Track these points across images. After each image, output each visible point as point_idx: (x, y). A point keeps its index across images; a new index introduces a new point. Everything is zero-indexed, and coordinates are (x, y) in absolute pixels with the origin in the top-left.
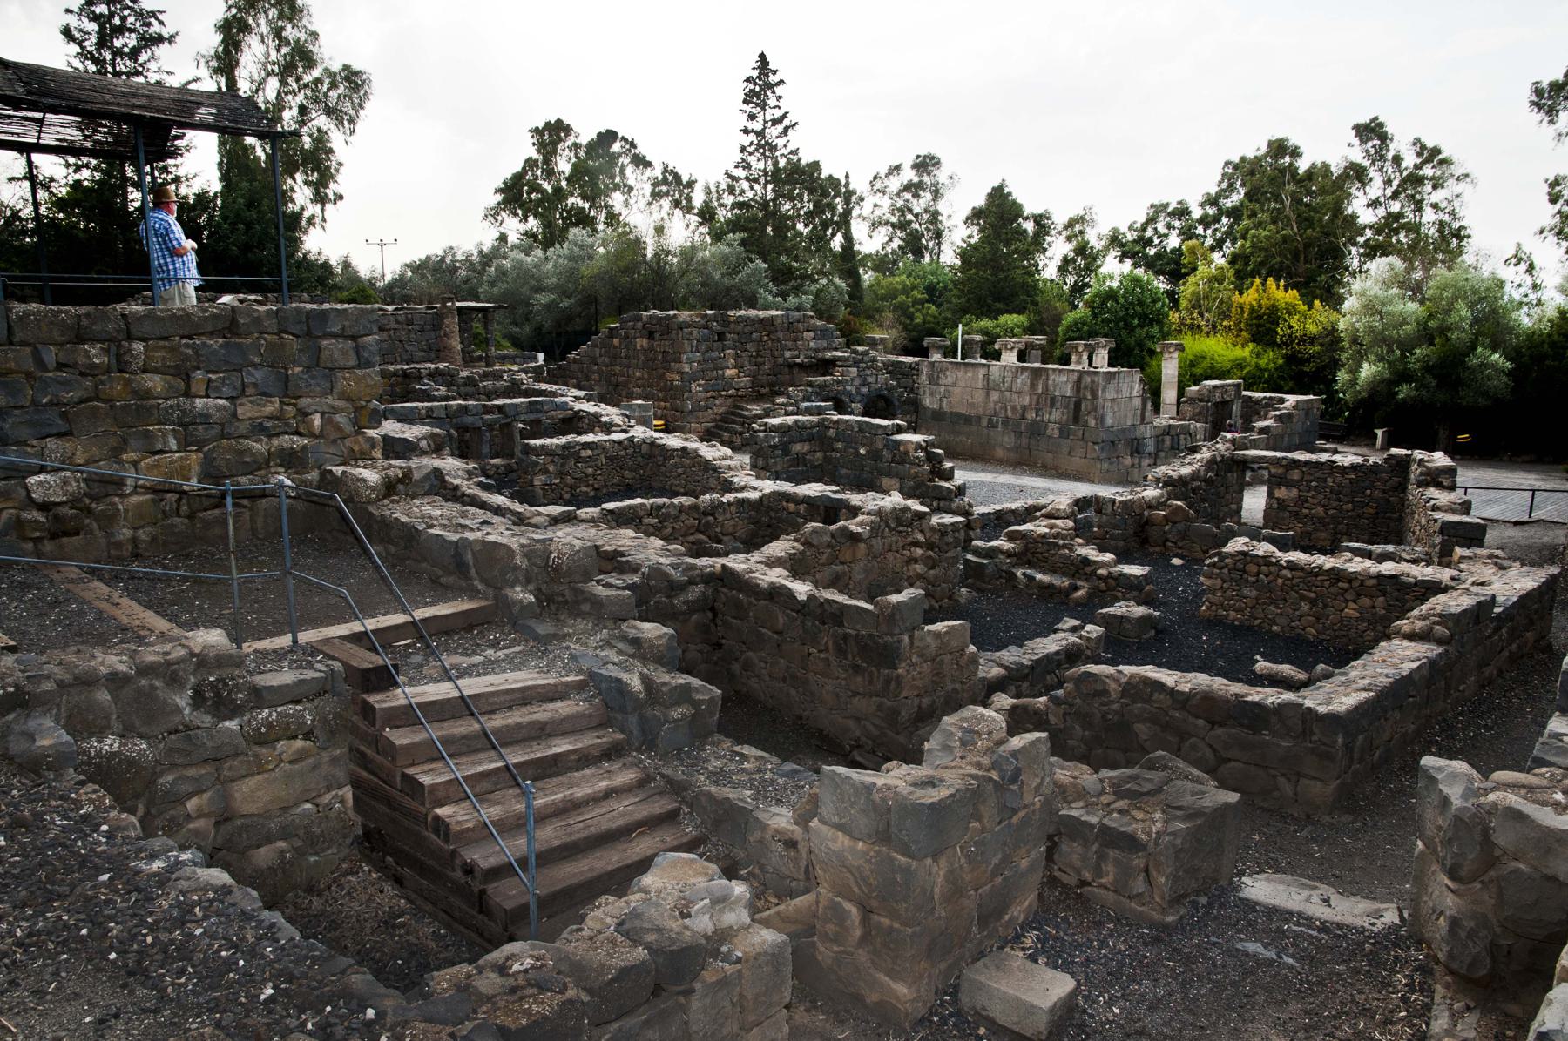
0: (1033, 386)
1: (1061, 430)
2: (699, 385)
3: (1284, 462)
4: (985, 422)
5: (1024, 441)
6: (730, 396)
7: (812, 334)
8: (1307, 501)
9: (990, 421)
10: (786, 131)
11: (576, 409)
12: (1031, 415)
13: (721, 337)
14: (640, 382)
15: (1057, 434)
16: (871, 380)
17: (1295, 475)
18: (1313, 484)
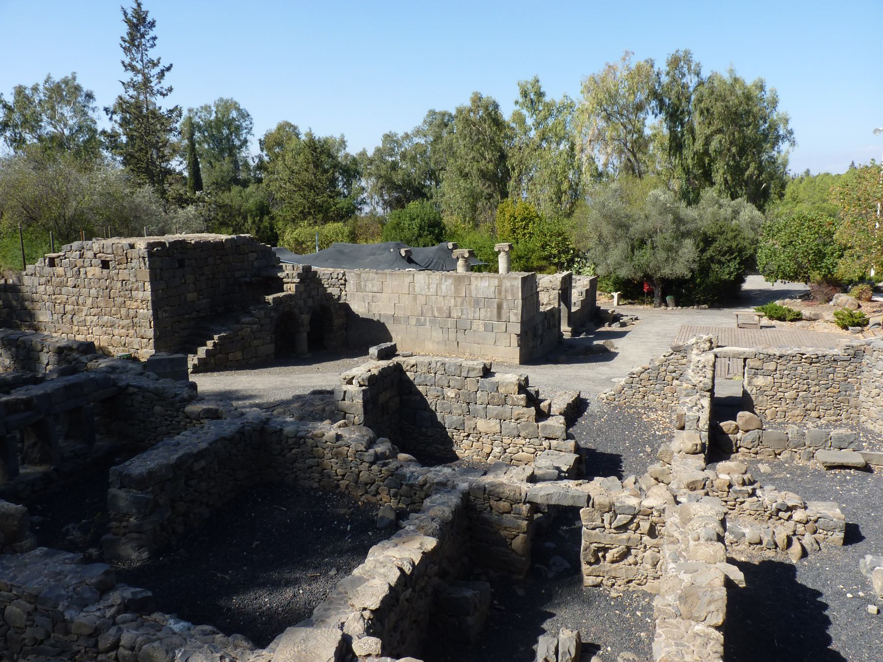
0: (457, 290)
1: (485, 325)
2: (165, 311)
3: (762, 356)
4: (413, 321)
5: (452, 336)
6: (193, 319)
7: (255, 255)
8: (781, 387)
9: (418, 320)
10: (161, 75)
11: (122, 384)
12: (455, 314)
13: (181, 264)
14: (94, 311)
15: (482, 328)
16: (314, 293)
17: (771, 366)
18: (786, 372)
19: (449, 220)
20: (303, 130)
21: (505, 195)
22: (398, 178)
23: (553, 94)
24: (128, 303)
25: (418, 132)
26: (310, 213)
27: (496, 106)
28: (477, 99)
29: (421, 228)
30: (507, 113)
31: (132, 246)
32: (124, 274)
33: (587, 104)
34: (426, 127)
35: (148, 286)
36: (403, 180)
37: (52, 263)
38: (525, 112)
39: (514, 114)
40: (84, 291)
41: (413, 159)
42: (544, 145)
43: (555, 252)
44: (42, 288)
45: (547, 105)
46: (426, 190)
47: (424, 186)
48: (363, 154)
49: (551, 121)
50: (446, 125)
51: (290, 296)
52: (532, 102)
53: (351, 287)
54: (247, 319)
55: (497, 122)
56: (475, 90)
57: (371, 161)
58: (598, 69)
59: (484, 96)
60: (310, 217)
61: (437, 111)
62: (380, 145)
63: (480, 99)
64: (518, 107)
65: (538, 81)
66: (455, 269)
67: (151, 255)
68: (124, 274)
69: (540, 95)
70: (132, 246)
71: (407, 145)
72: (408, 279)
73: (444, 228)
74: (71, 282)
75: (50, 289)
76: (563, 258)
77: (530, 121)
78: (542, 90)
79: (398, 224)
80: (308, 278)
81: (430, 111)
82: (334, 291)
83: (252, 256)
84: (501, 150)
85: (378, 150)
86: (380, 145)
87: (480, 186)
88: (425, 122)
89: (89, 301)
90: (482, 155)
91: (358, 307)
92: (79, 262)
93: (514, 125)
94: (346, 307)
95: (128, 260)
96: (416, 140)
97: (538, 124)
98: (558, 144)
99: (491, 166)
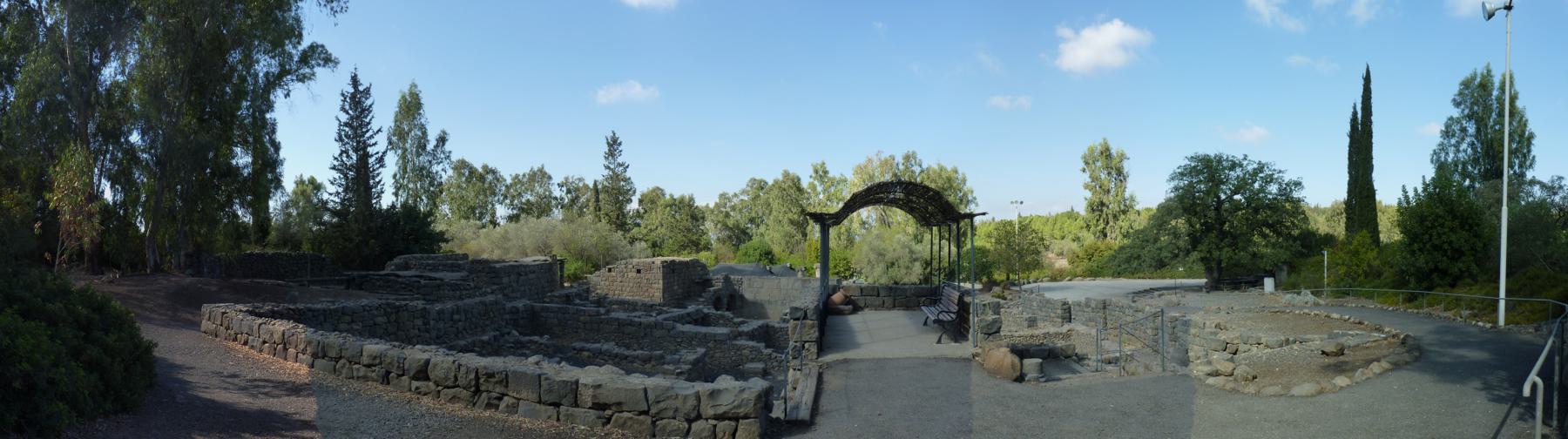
13: (673, 272)
19: (776, 250)
20: (668, 192)
21: (805, 235)
22: (730, 222)
23: (834, 173)
24: (650, 290)
25: (744, 192)
26: (688, 246)
27: (799, 179)
28: (786, 174)
29: (760, 255)
30: (805, 184)
31: (653, 263)
32: (649, 276)
33: (856, 181)
34: (749, 189)
35: (661, 282)
36: (734, 225)
37: (610, 270)
38: (816, 182)
39: (810, 183)
40: (626, 284)
41: (740, 211)
42: (829, 203)
43: (842, 269)
44: (603, 282)
45: (829, 179)
46: (748, 231)
47: (747, 228)
48: (707, 206)
49: (833, 189)
50: (762, 188)
51: (719, 289)
52: (821, 176)
53: (745, 285)
54: (701, 300)
55: (800, 190)
56: (785, 168)
57: (712, 211)
58: (862, 161)
59: (791, 172)
60: (688, 248)
61: (757, 178)
62: (718, 201)
63: (788, 174)
64: (811, 180)
65: (824, 164)
66: (796, 275)
67: (663, 267)
68: (649, 276)
69: (826, 172)
70: (653, 263)
71: (735, 200)
72: (777, 281)
73: (773, 255)
74: (619, 279)
75: (607, 283)
76: (847, 274)
77: (819, 189)
78: (827, 169)
79: (746, 253)
80: (727, 279)
81: (751, 180)
82: (736, 287)
83: (699, 268)
84: (801, 206)
85: (716, 204)
86: (718, 201)
87: (791, 229)
88: (748, 185)
89: (628, 289)
90: (790, 209)
91: (748, 296)
92: (625, 270)
93: (809, 191)
94: (742, 297)
95: (651, 269)
96: (742, 197)
97: (825, 191)
98: (838, 203)
99: (796, 217)
